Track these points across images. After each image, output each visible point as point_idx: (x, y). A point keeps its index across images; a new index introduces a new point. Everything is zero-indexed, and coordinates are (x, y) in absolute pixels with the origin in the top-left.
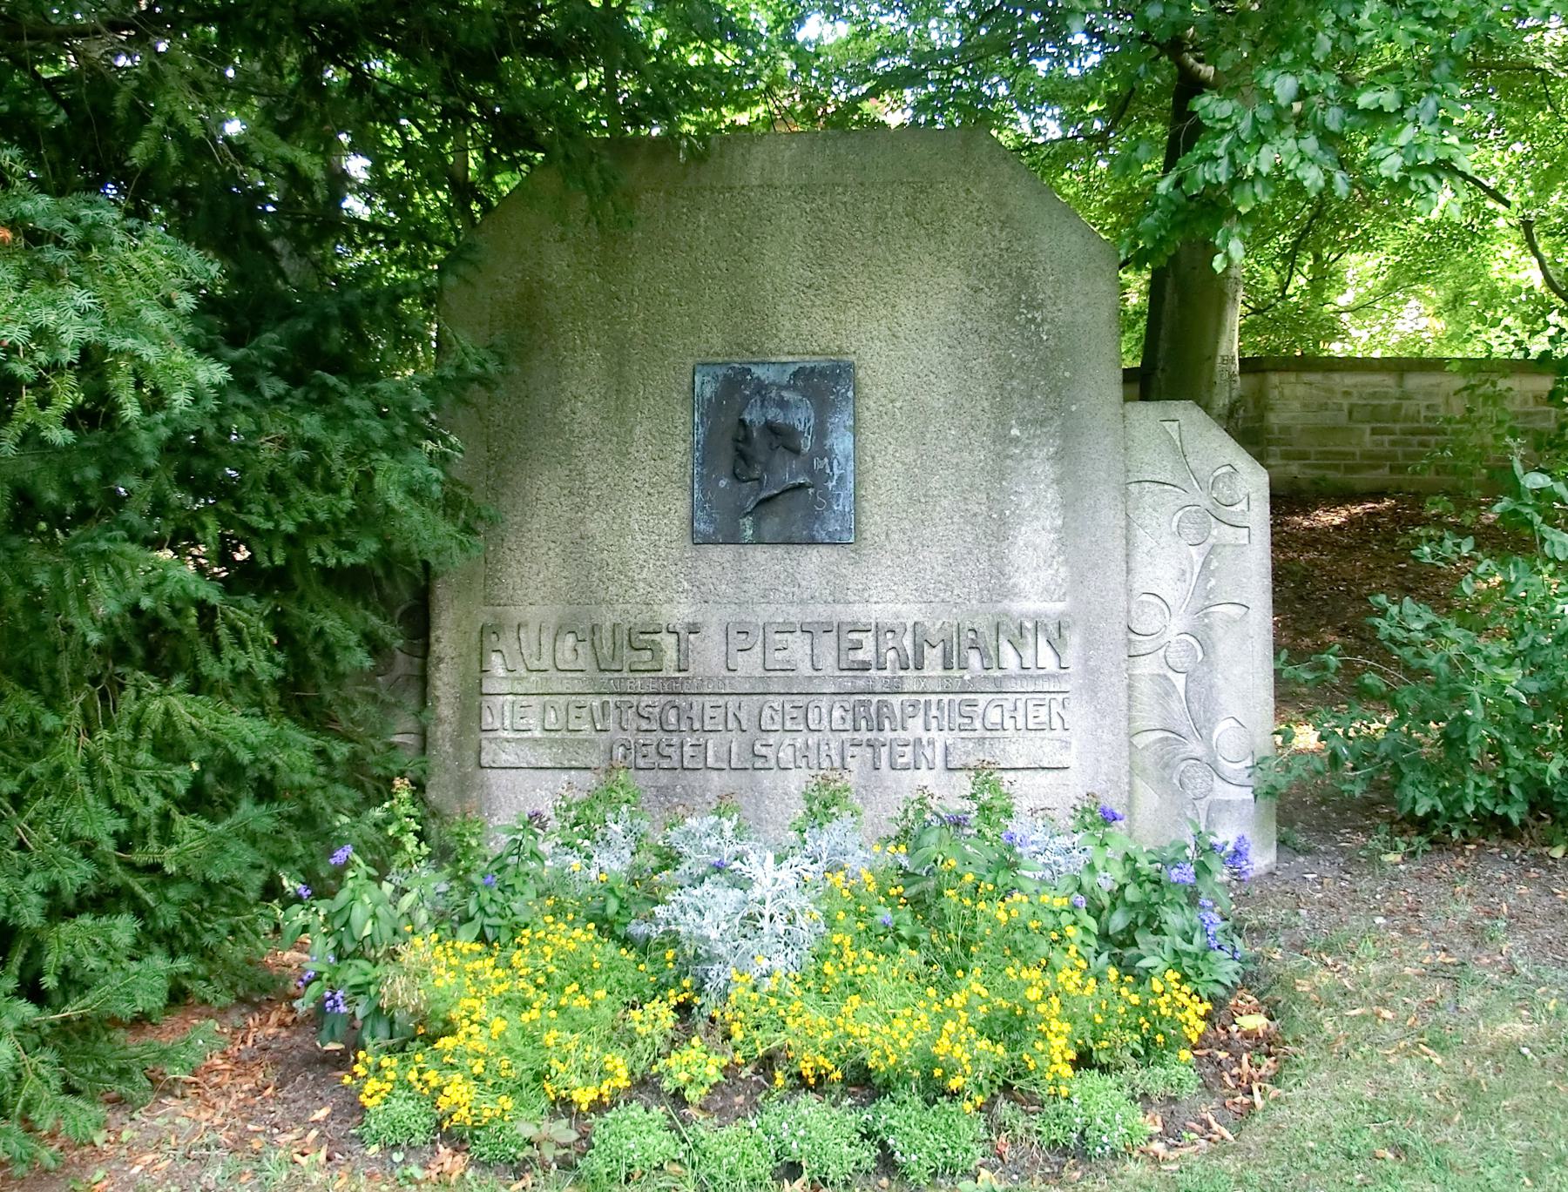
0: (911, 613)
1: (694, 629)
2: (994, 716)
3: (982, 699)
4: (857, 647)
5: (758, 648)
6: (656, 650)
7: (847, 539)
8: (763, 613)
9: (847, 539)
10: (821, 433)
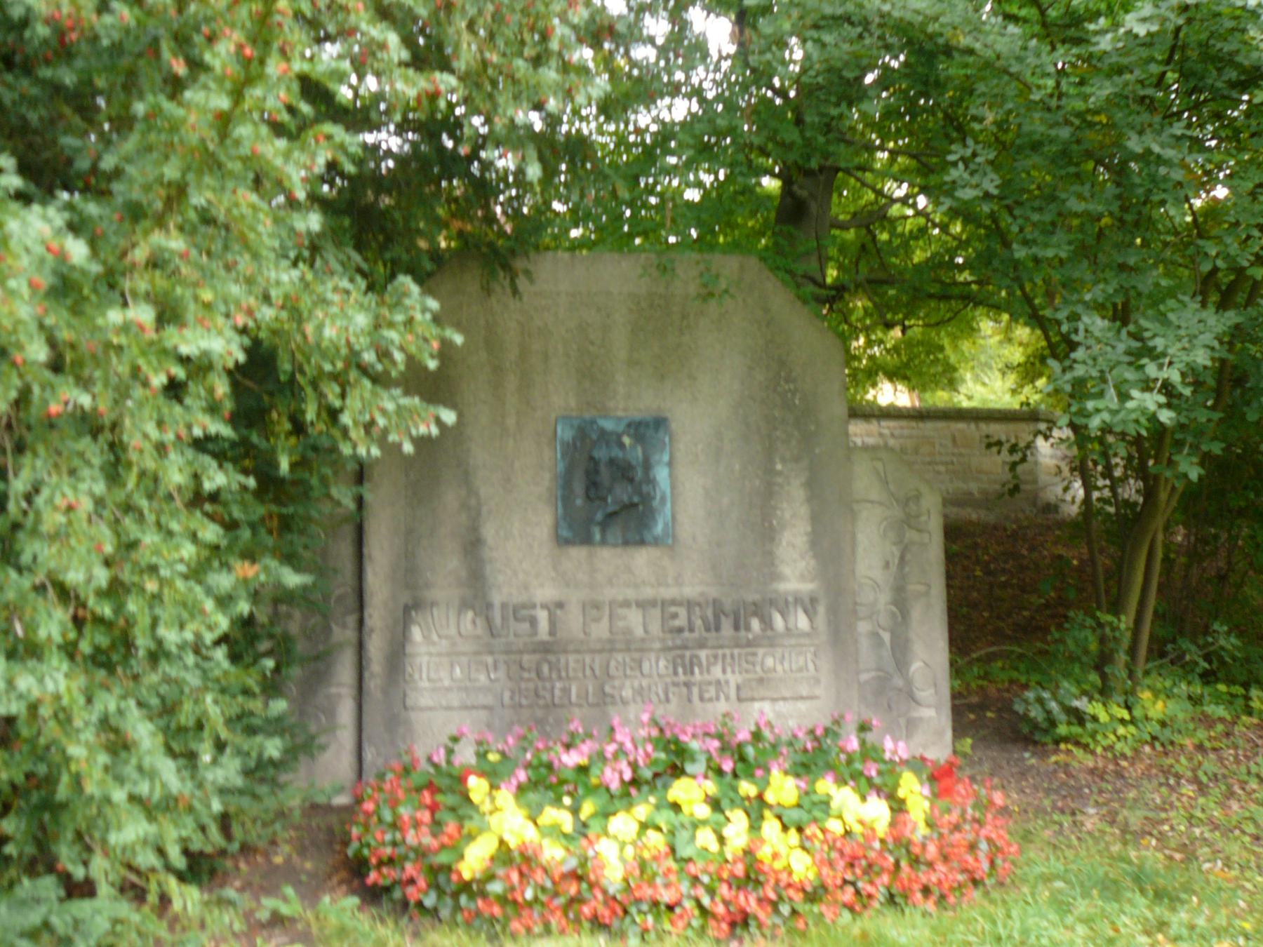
0: (713, 592)
1: (560, 605)
3: (761, 651)
4: (675, 616)
5: (606, 620)
6: (533, 622)
8: (609, 593)
10: (647, 465)
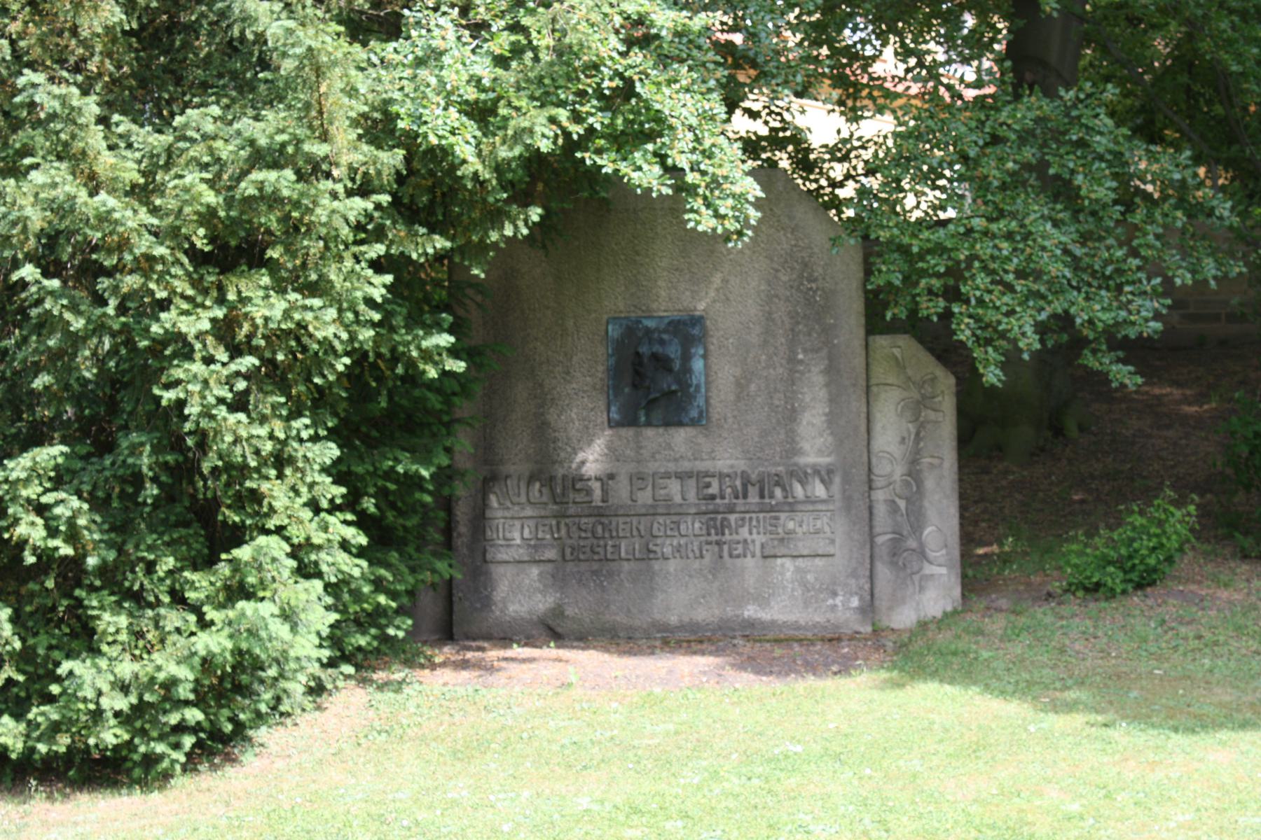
0: (741, 465)
2: (791, 525)
3: (783, 516)
4: (708, 485)
8: (652, 467)
9: (700, 421)
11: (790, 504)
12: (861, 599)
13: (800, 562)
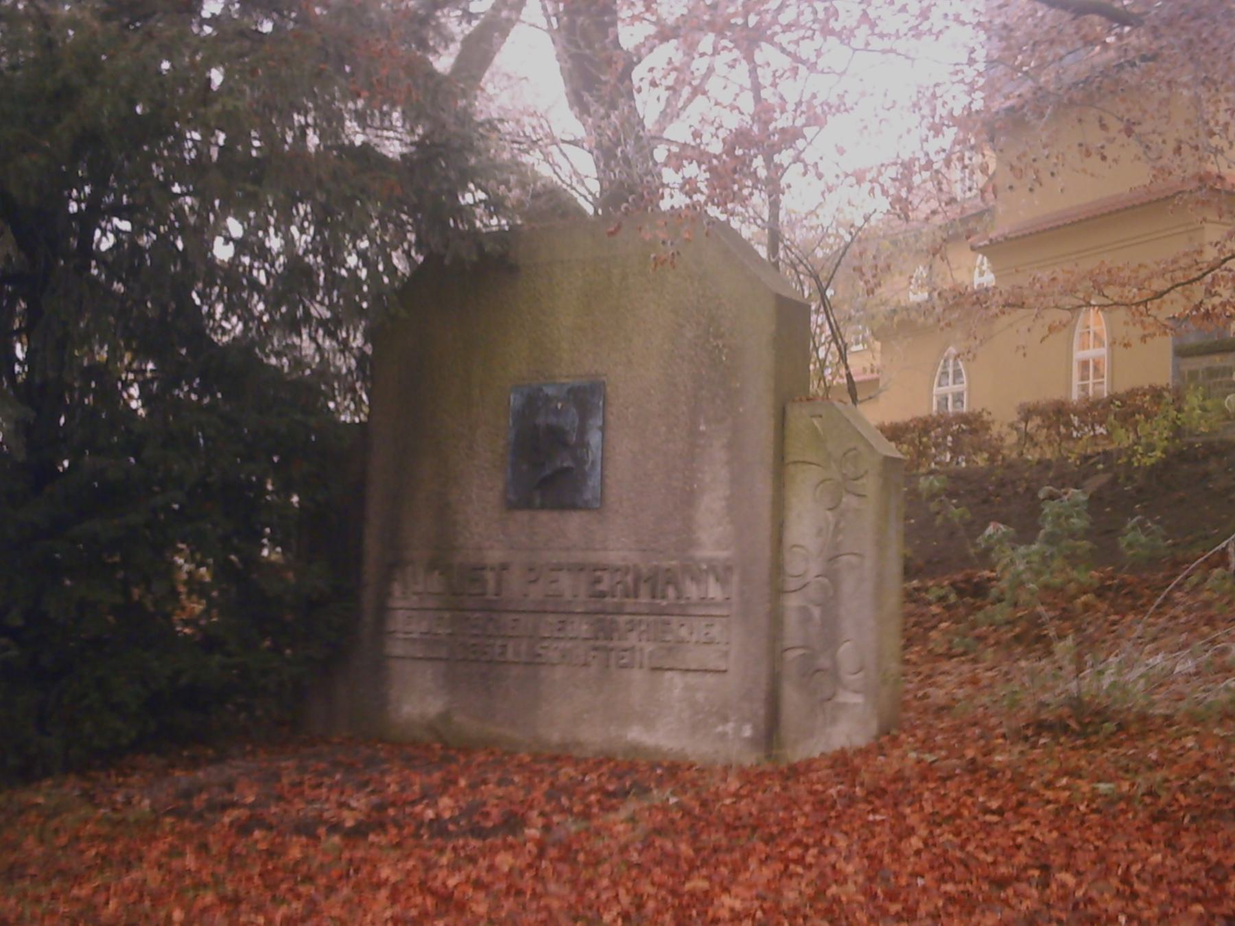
0: (634, 558)
1: (504, 567)
2: (683, 632)
3: (675, 619)
4: (598, 581)
7: (596, 508)
9: (596, 508)
10: (582, 431)
11: (681, 606)
12: (755, 728)
13: (691, 679)
